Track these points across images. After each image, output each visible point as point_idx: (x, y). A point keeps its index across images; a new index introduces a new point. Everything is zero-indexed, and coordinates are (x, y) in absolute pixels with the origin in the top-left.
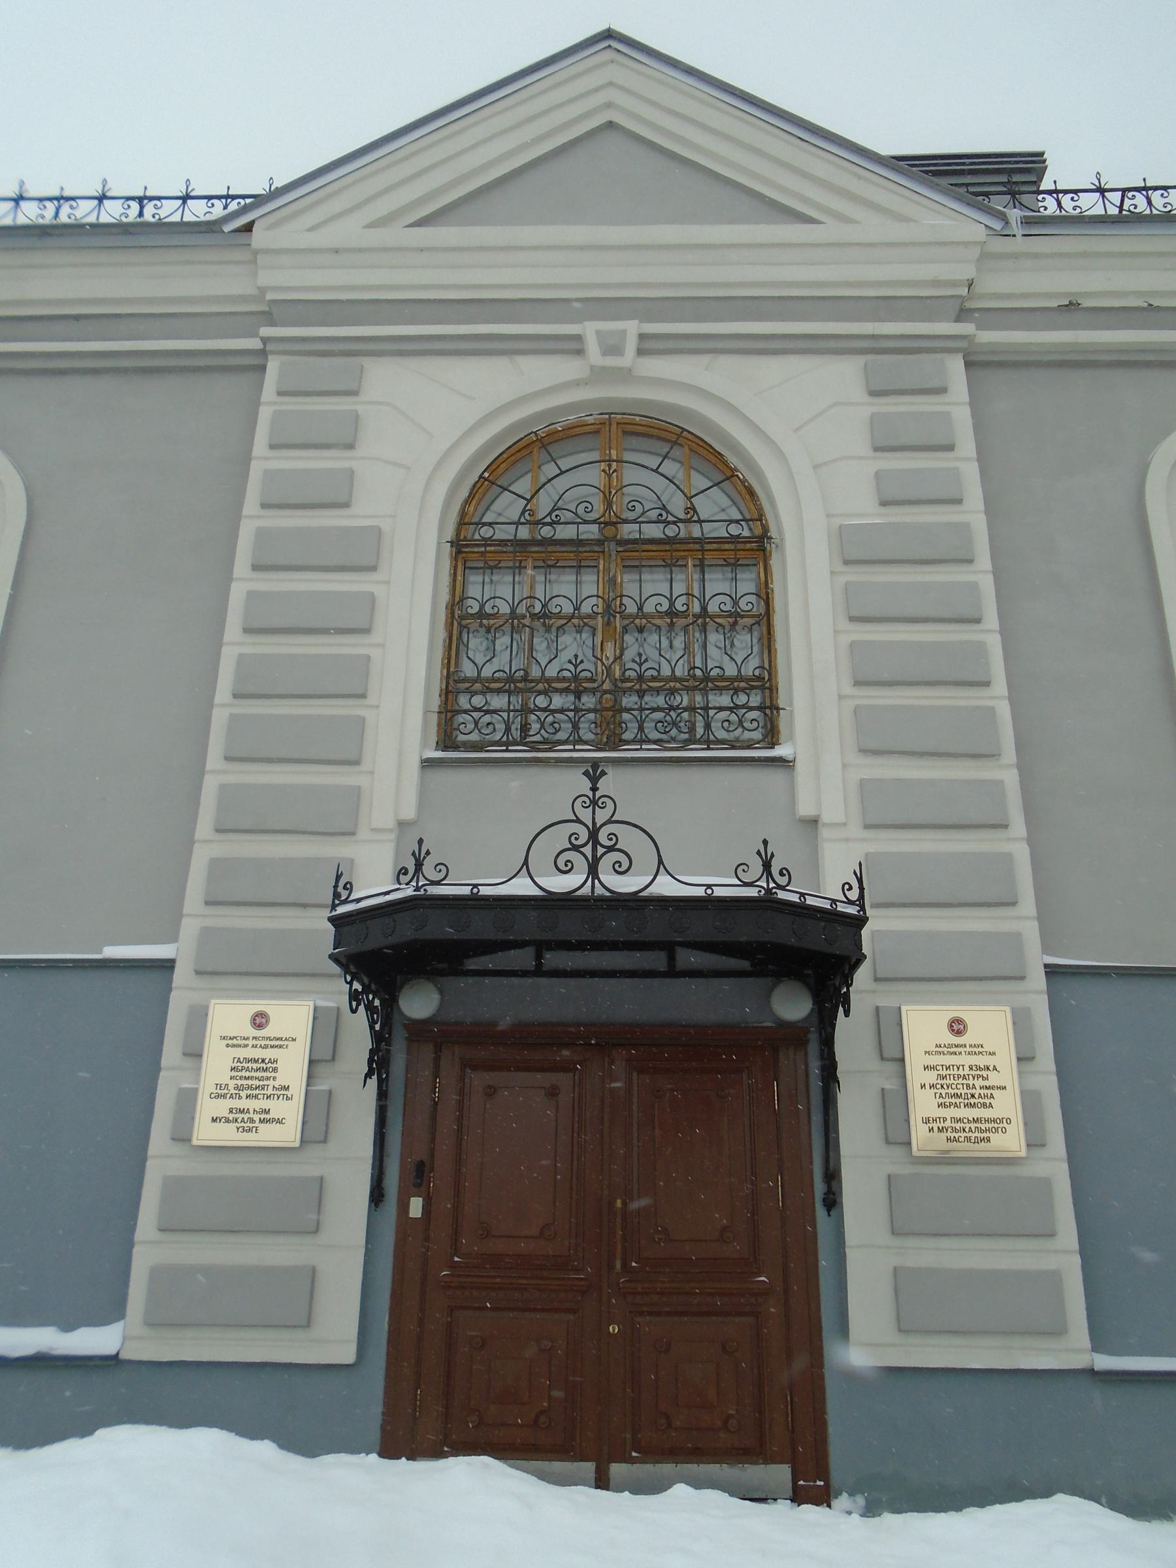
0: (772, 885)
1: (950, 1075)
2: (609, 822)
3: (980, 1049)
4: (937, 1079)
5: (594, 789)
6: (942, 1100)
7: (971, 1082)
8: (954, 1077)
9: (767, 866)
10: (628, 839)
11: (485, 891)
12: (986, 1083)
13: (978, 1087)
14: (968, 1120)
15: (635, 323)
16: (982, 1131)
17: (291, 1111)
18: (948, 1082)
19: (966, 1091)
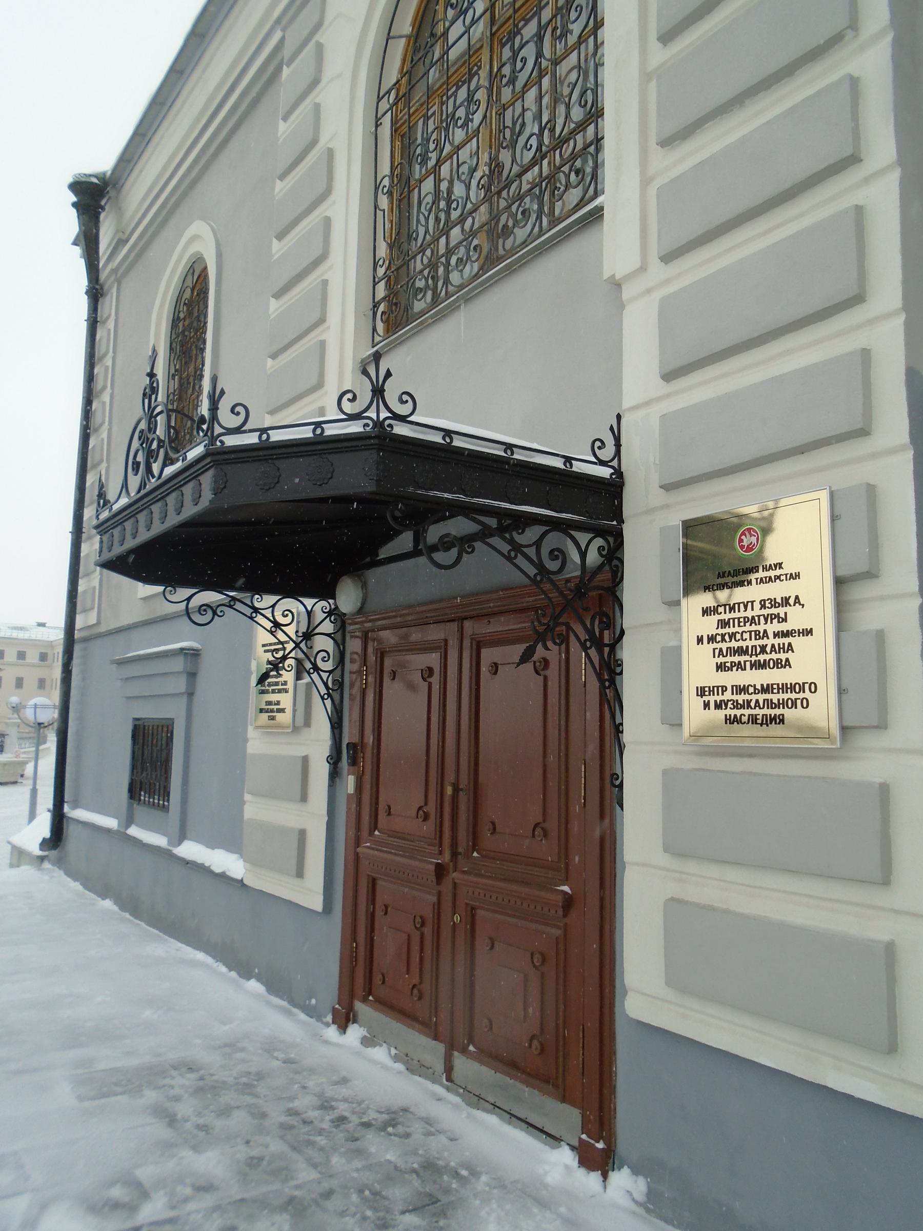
0: (384, 414)
1: (734, 619)
3: (778, 572)
4: (717, 628)
6: (722, 660)
7: (761, 628)
8: (739, 622)
12: (784, 627)
13: (771, 635)
14: (755, 689)
16: (770, 704)
18: (731, 630)
19: (754, 642)
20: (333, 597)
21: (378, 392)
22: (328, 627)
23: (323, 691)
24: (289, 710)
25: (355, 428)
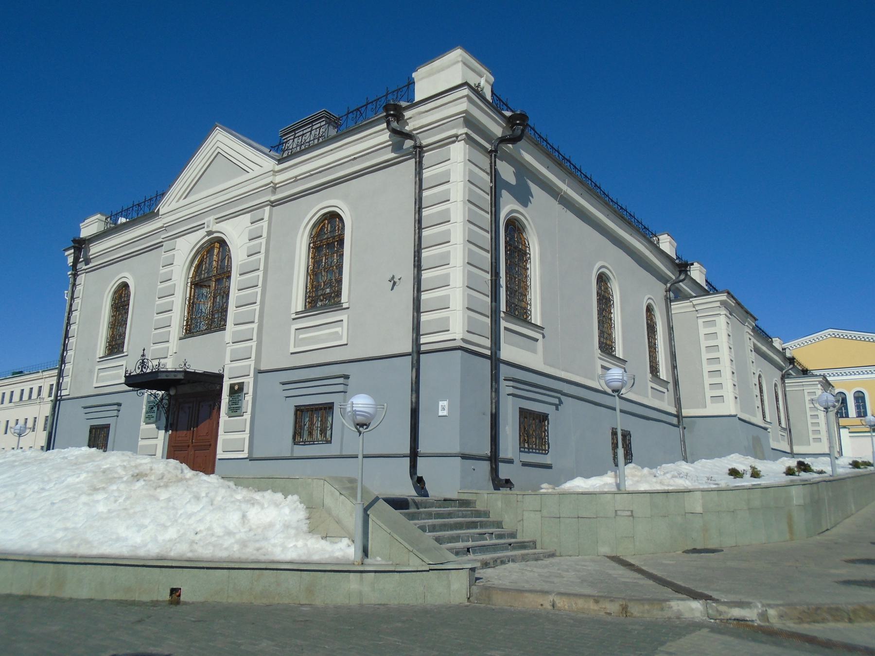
15: (212, 217)
17: (154, 415)
20: (169, 391)
21: (185, 365)
22: (167, 398)
23: (165, 412)
24: (155, 417)
25: (181, 370)
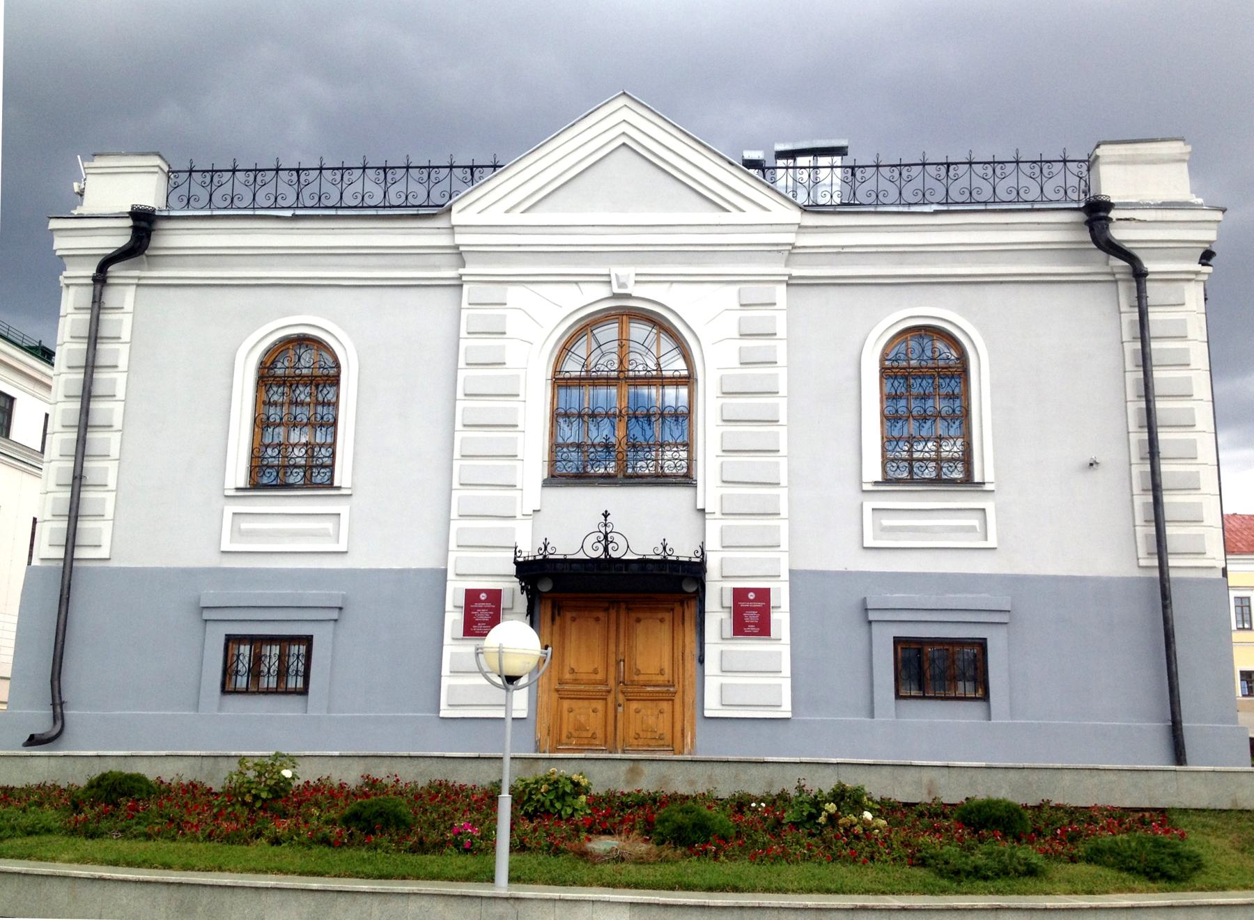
2: (611, 532)
5: (606, 520)
9: (664, 548)
10: (617, 538)
11: (568, 557)
